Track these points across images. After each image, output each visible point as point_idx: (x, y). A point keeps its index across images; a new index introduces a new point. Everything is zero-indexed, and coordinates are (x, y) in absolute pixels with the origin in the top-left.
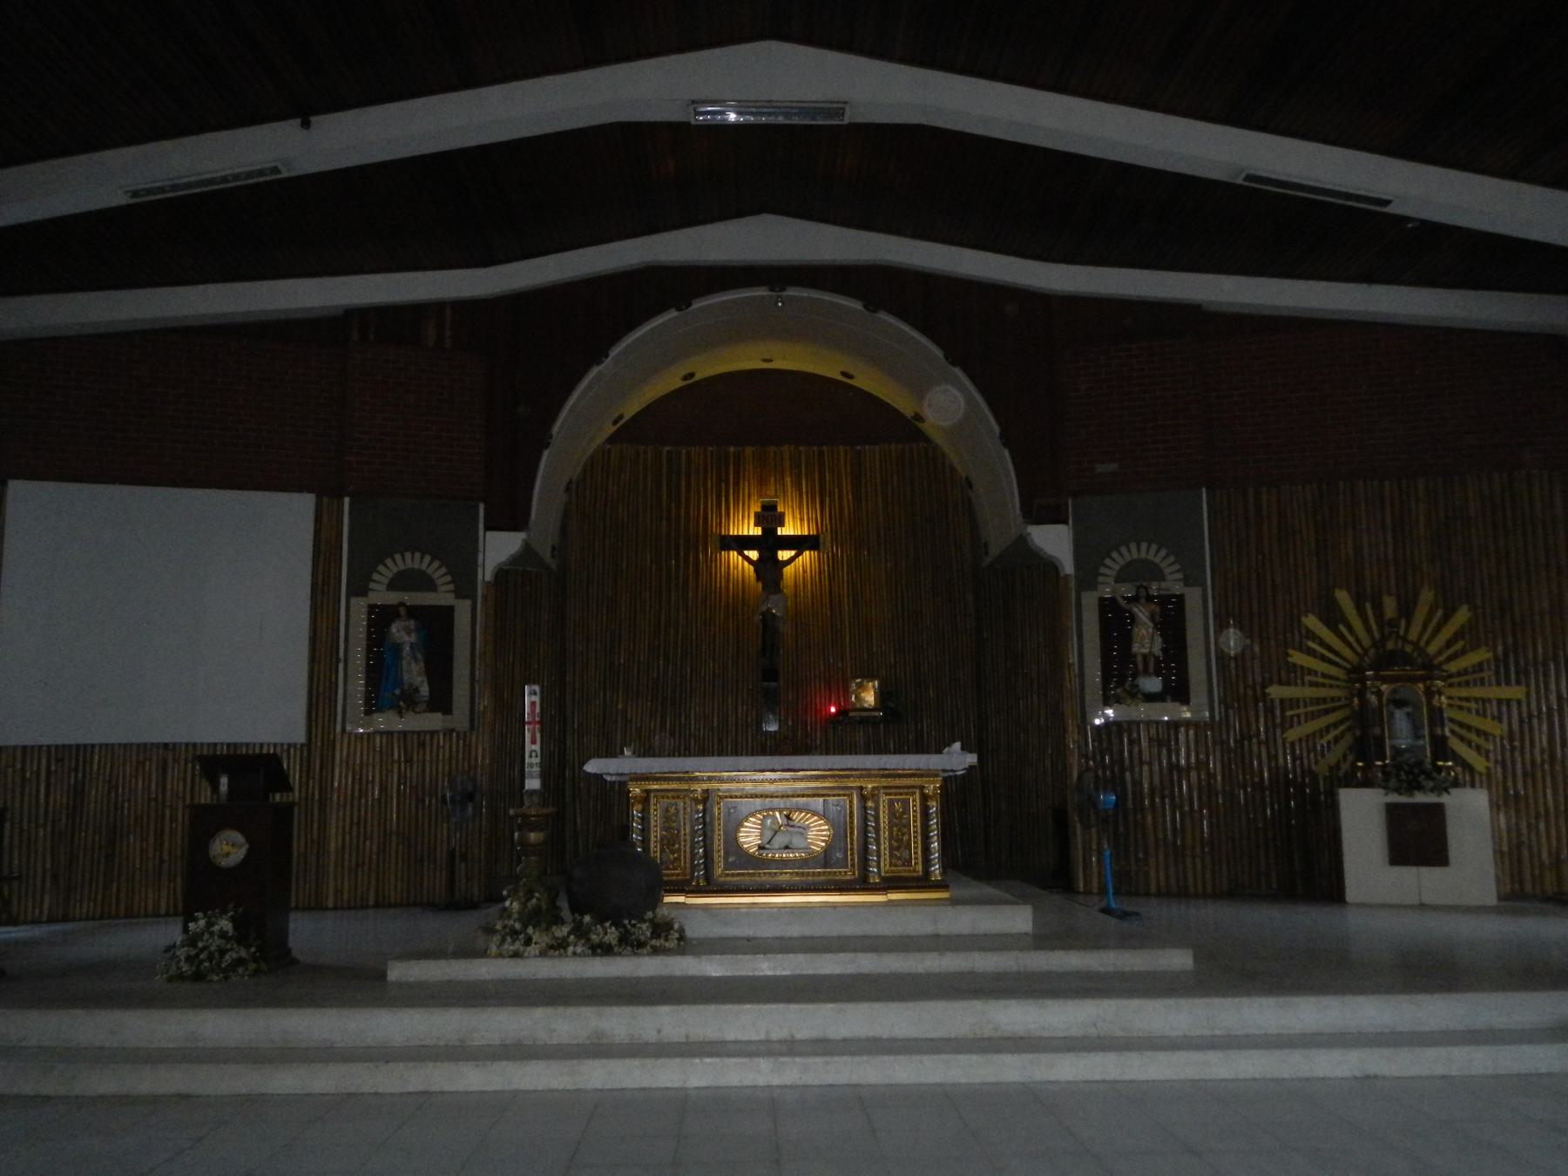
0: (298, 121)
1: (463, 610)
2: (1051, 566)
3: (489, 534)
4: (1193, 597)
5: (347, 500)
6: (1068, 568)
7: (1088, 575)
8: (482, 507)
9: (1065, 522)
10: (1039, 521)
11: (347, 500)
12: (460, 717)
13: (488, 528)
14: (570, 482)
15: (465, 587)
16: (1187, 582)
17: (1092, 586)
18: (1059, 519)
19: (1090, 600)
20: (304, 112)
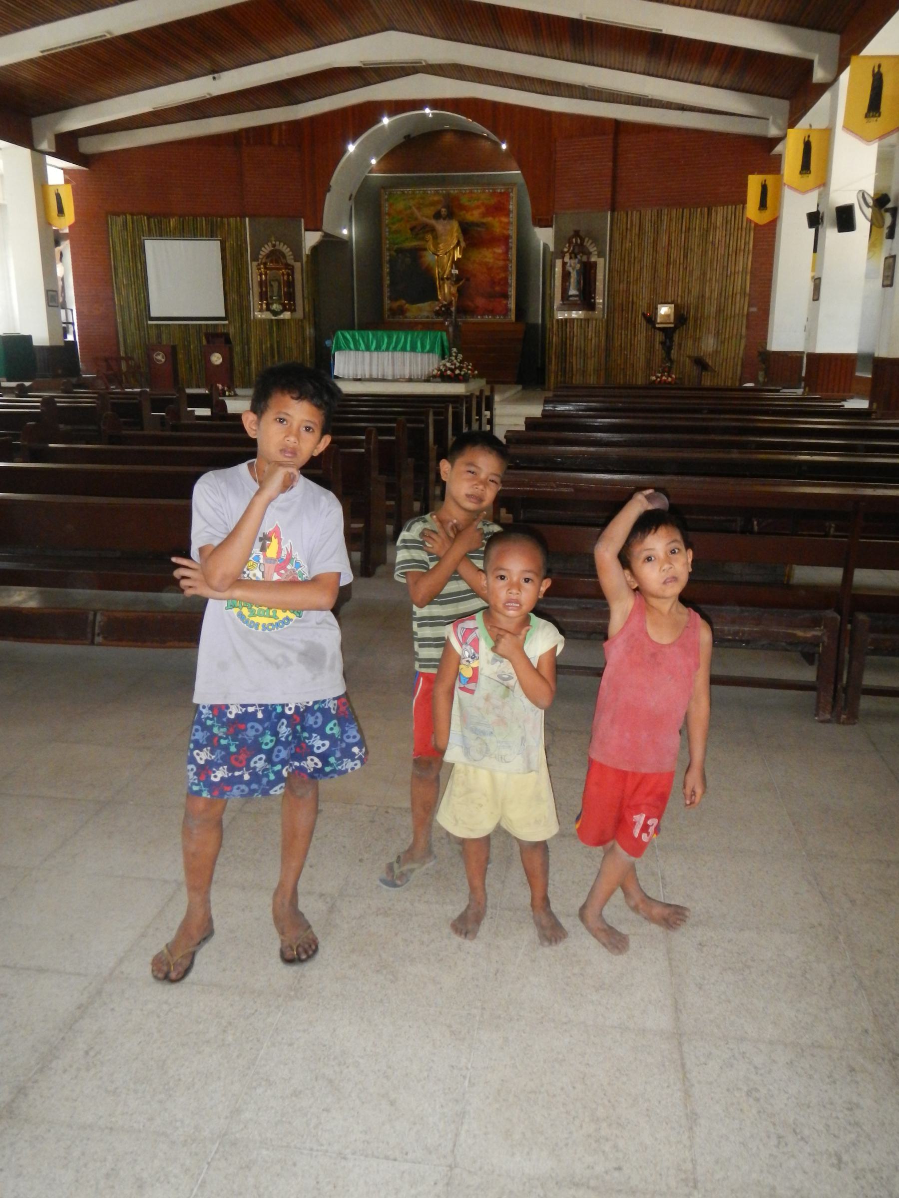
0: (211, 77)
1: (297, 265)
3: (307, 233)
4: (601, 262)
5: (247, 219)
8: (303, 220)
9: (551, 226)
11: (247, 219)
12: (299, 314)
13: (306, 230)
14: (351, 195)
15: (298, 257)
16: (601, 254)
18: (548, 225)
19: (559, 263)
20: (215, 70)
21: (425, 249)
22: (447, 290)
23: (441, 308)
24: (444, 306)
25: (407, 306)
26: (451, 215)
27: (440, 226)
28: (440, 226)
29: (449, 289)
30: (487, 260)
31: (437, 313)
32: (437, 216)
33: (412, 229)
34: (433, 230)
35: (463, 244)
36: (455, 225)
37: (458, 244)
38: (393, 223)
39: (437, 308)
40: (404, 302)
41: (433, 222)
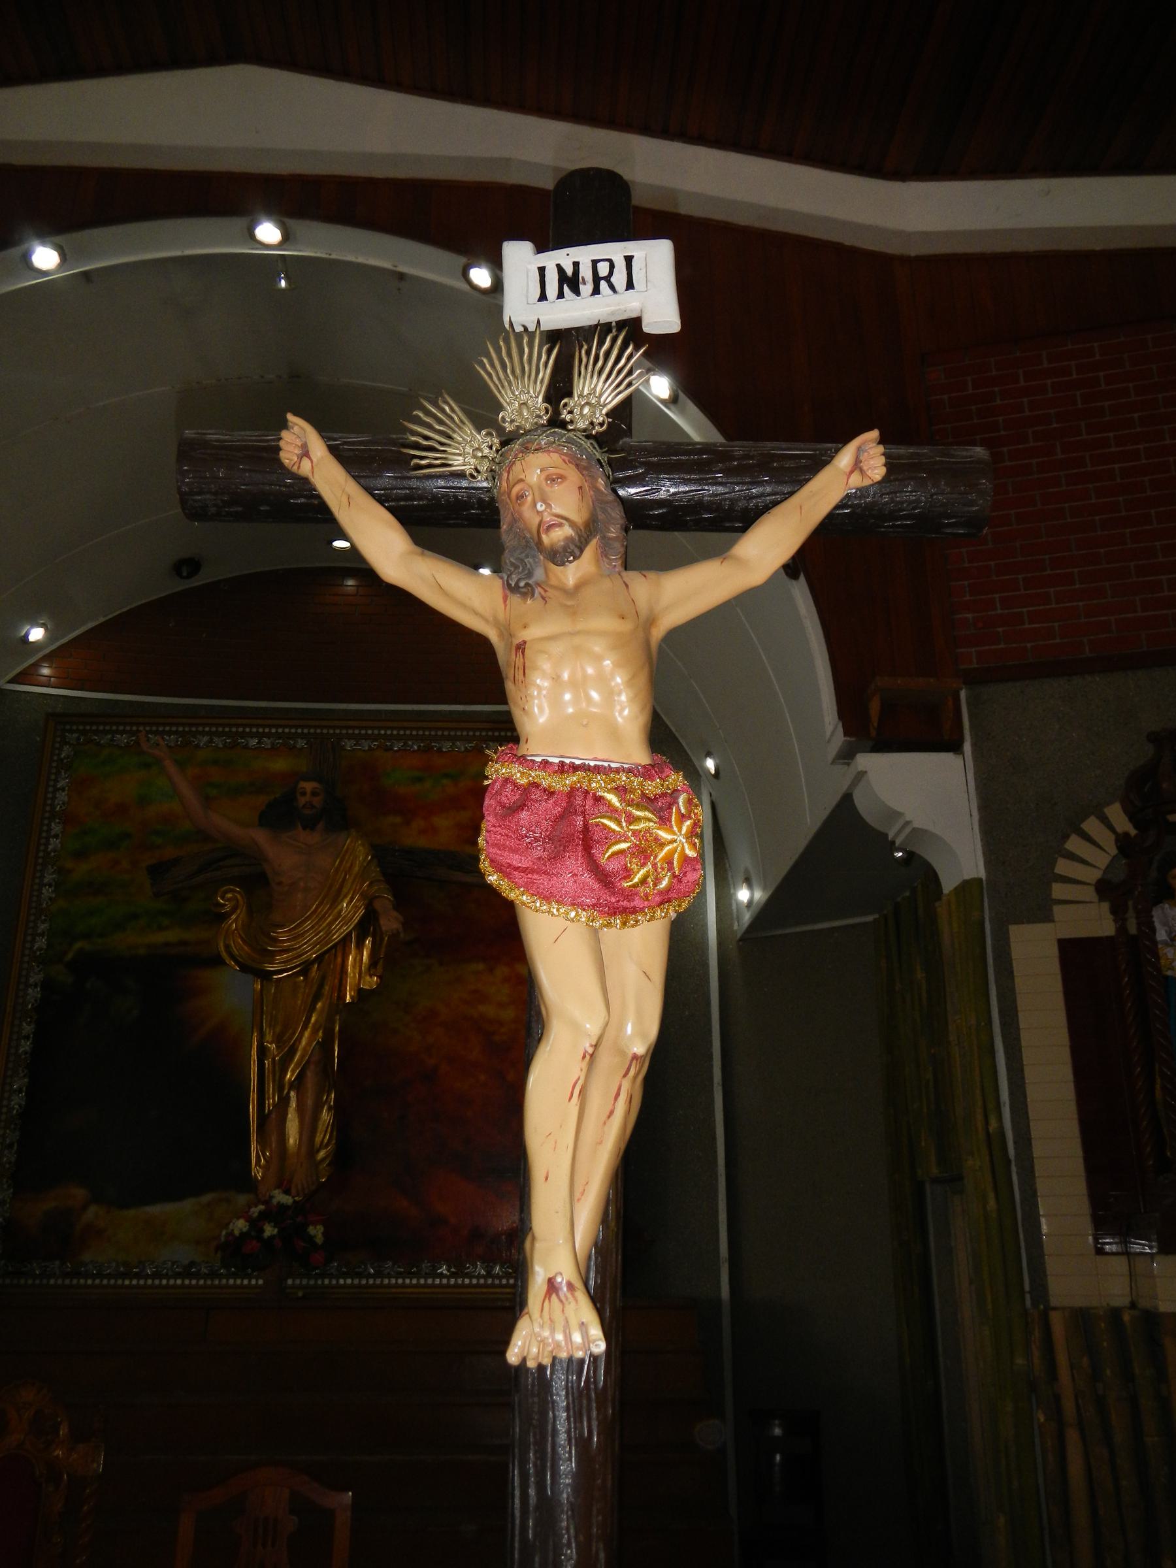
2: (920, 873)
6: (962, 858)
7: (1021, 882)
9: (954, 747)
10: (882, 745)
17: (1041, 911)
18: (935, 736)
19: (1034, 953)
21: (216, 961)
22: (295, 1129)
23: (255, 1225)
24: (275, 1214)
25: (92, 1212)
26: (335, 817)
27: (284, 855)
28: (284, 855)
29: (309, 1127)
30: (489, 1010)
31: (235, 1253)
32: (281, 814)
33: (157, 871)
34: (257, 881)
35: (390, 922)
36: (359, 852)
37: (367, 925)
38: (80, 855)
39: (240, 1225)
40: (79, 1193)
41: (261, 837)
